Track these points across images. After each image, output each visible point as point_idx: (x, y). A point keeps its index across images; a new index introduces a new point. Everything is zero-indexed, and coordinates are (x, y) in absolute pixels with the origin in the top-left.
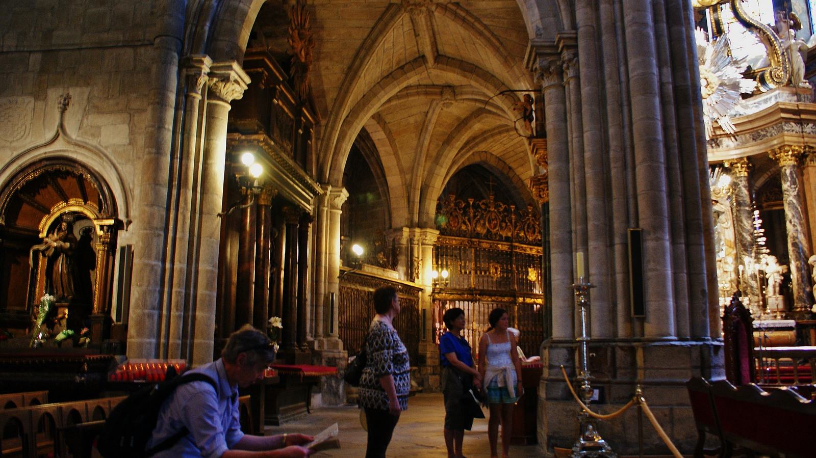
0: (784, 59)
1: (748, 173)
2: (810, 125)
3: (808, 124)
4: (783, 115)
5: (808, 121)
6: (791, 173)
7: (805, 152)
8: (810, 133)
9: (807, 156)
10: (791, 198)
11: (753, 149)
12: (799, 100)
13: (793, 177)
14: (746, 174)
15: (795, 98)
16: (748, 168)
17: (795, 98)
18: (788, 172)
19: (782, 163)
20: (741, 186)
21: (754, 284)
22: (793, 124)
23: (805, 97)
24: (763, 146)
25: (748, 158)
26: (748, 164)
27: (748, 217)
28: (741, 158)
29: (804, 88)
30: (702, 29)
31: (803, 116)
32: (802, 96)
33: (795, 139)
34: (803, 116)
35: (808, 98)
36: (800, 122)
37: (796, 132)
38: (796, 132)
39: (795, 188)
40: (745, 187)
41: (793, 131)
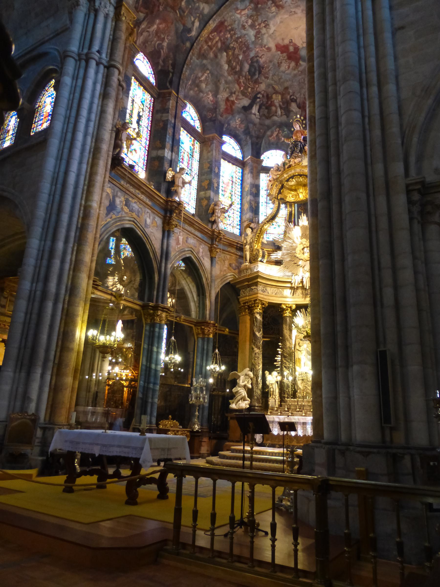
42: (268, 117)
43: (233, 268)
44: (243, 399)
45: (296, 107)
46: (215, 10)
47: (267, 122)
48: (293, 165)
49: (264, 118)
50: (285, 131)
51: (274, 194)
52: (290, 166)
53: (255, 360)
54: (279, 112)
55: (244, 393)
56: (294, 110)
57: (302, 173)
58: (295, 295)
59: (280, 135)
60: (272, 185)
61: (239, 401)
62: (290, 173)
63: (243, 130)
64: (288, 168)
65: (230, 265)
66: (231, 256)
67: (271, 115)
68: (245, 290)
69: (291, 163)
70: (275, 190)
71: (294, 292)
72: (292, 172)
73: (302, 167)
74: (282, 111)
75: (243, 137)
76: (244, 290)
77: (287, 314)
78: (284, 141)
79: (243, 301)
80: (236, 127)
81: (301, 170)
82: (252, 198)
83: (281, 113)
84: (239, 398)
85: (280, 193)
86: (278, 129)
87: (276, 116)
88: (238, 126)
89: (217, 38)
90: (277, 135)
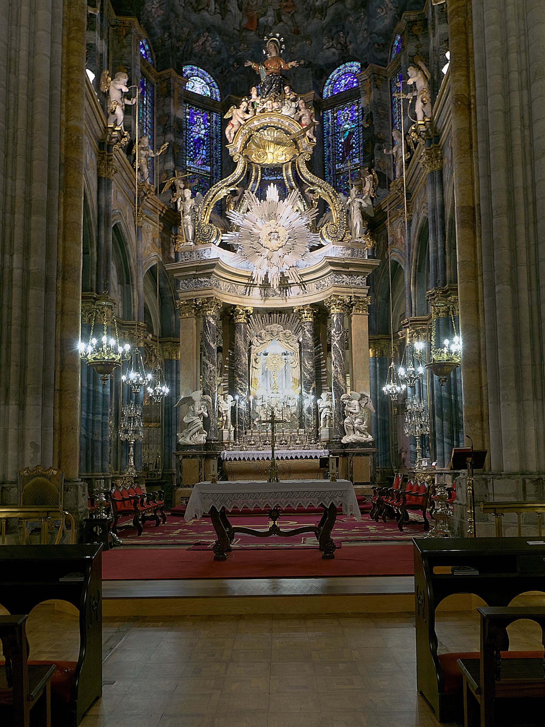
0: (343, 215)
1: (314, 319)
3: (358, 276)
5: (358, 274)
6: (337, 319)
8: (359, 284)
10: (335, 343)
13: (338, 323)
14: (311, 319)
15: (349, 252)
17: (349, 252)
18: (335, 319)
19: (332, 311)
20: (305, 330)
22: (344, 276)
23: (358, 252)
25: (312, 305)
26: (313, 311)
27: (309, 358)
30: (275, 186)
31: (351, 269)
34: (351, 269)
35: (361, 251)
36: (350, 274)
37: (346, 283)
38: (346, 283)
39: (339, 334)
41: (343, 282)
42: (197, 10)
43: (156, 245)
45: (236, 7)
47: (194, 17)
48: (270, 110)
49: (190, 8)
50: (217, 41)
51: (239, 147)
52: (263, 110)
53: (210, 380)
54: (213, 7)
56: (233, 11)
57: (280, 126)
58: (251, 294)
59: (208, 44)
60: (235, 133)
62: (263, 121)
63: (159, 19)
64: (260, 112)
66: (153, 225)
67: (200, 7)
68: (189, 282)
69: (265, 106)
70: (240, 141)
71: (250, 291)
72: (266, 120)
73: (283, 116)
74: (217, 6)
75: (158, 30)
76: (187, 282)
78: (251, 66)
79: (186, 297)
80: (151, 10)
81: (279, 120)
83: (215, 8)
85: (245, 147)
86: (207, 34)
87: (207, 10)
88: (153, 10)
90: (204, 43)
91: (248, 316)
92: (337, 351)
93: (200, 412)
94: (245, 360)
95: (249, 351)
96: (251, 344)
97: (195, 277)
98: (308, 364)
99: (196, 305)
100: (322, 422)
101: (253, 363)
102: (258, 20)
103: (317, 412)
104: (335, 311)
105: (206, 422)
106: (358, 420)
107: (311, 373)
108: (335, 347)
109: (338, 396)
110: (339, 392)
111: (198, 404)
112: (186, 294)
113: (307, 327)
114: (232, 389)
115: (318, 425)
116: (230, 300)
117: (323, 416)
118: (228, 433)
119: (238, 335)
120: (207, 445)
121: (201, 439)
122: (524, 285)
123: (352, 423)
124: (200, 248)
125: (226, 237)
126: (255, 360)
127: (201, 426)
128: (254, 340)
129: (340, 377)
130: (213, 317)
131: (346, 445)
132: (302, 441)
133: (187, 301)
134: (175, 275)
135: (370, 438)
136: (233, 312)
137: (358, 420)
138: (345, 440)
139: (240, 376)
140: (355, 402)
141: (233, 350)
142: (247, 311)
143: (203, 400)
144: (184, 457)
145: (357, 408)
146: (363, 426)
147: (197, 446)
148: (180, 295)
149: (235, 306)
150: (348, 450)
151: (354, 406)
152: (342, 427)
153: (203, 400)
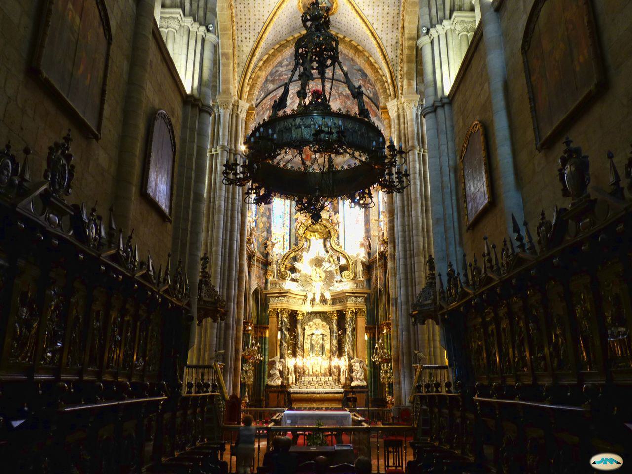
1: (338, 318)
2: (361, 298)
4: (347, 294)
5: (360, 297)
7: (356, 311)
9: (357, 313)
11: (338, 307)
12: (357, 287)
14: (336, 318)
15: (356, 285)
16: (338, 315)
21: (335, 370)
22: (353, 298)
24: (341, 306)
25: (337, 311)
28: (334, 311)
29: (360, 281)
31: (356, 295)
32: (359, 285)
33: (353, 305)
34: (356, 295)
40: (335, 324)
44: (278, 378)
46: (275, 88)
55: (278, 373)
61: (276, 379)
65: (256, 275)
77: (300, 317)
82: (266, 220)
84: (276, 378)
85: (304, 233)
89: (269, 103)
91: (303, 315)
92: (349, 337)
93: (279, 368)
94: (301, 338)
95: (304, 333)
96: (304, 330)
97: (277, 297)
98: (335, 342)
99: (278, 311)
100: (341, 373)
101: (305, 340)
102: (311, 156)
103: (339, 369)
104: (349, 316)
105: (281, 373)
106: (359, 374)
107: (336, 347)
108: (348, 335)
109: (349, 361)
110: (350, 358)
111: (278, 363)
112: (272, 305)
113: (334, 322)
114: (294, 355)
115: (339, 375)
116: (294, 308)
117: (342, 371)
118: (292, 378)
119: (298, 326)
120: (282, 385)
121: (279, 382)
122: (412, 333)
123: (357, 376)
124: (281, 282)
125: (293, 276)
126: (307, 339)
127: (279, 375)
128: (306, 327)
129: (351, 351)
130: (286, 318)
131: (354, 387)
132: (331, 385)
133: (273, 309)
134: (267, 295)
135: (365, 383)
136: (296, 313)
137: (359, 374)
138: (353, 384)
139: (298, 348)
140: (358, 364)
141: (295, 333)
142: (303, 313)
143: (280, 362)
144: (271, 392)
145: (359, 367)
146: (362, 377)
147: (277, 386)
148: (269, 306)
149: (297, 311)
150: (354, 389)
151: (357, 367)
152: (351, 377)
153: (280, 362)
